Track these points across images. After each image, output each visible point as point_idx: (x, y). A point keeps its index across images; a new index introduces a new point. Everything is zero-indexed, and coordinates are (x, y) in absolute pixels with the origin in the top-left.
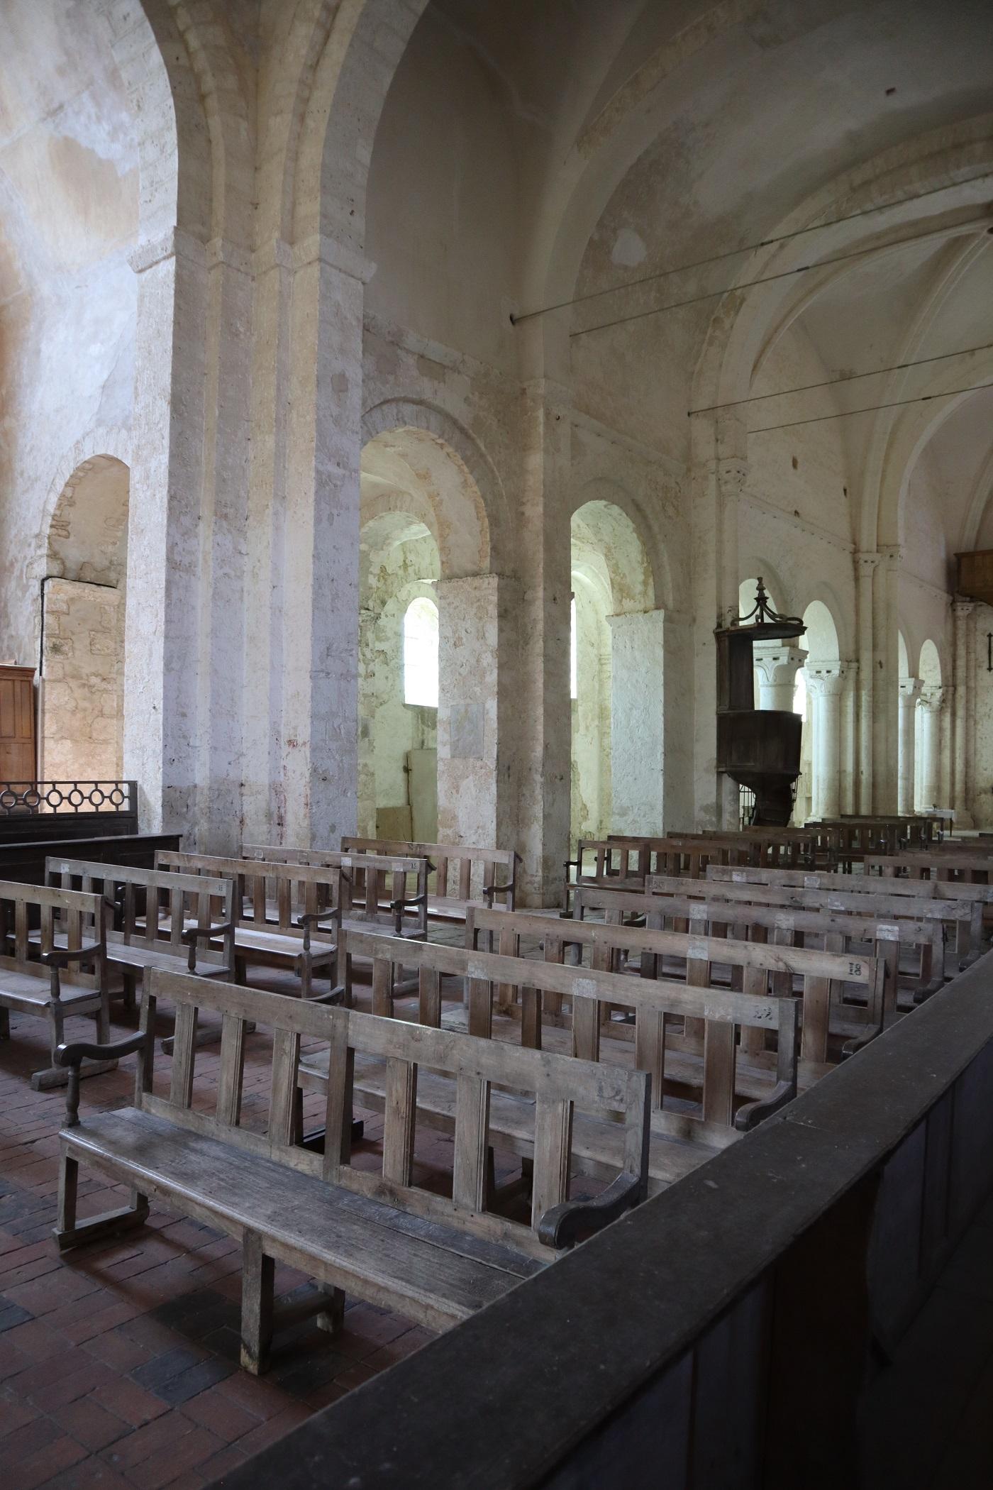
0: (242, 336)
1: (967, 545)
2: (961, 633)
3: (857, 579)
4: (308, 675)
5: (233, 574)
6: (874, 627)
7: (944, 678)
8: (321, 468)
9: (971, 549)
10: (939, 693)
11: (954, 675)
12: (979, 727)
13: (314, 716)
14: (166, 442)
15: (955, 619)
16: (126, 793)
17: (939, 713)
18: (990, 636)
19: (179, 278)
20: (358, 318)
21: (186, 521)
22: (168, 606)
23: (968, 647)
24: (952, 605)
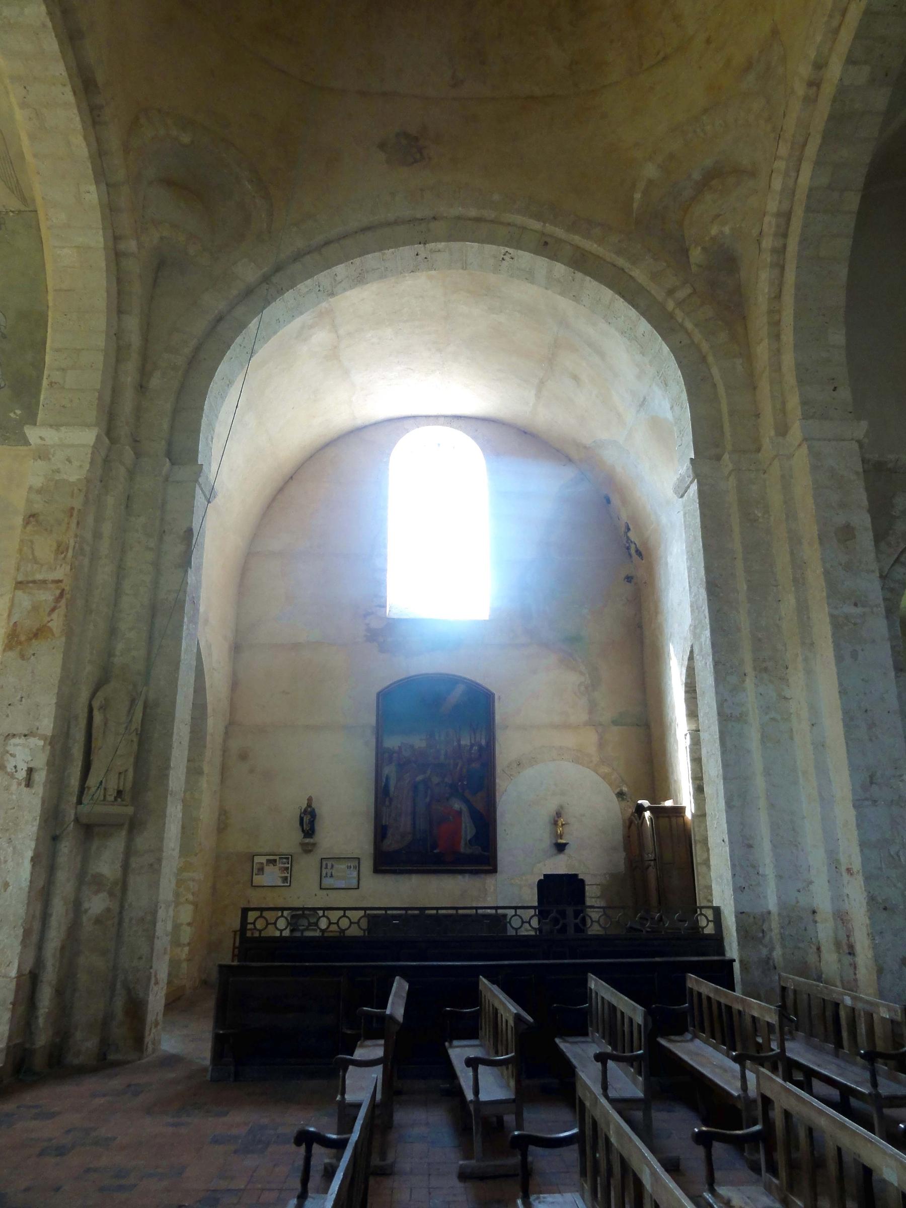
0: (761, 520)
4: (850, 805)
5: (779, 717)
8: (836, 612)
13: (863, 845)
14: (707, 621)
16: (711, 918)
19: (701, 493)
20: (857, 473)
21: (733, 679)
22: (723, 753)
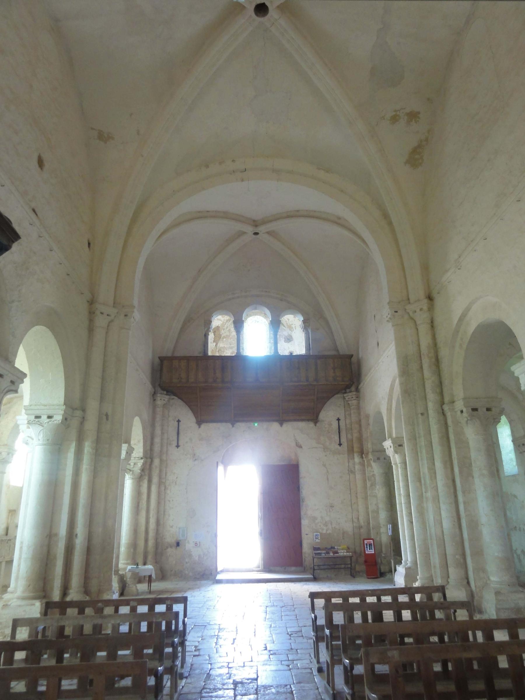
1: (167, 351)
2: (158, 418)
3: (91, 330)
6: (103, 378)
7: (145, 452)
9: (169, 354)
10: (140, 463)
11: (151, 450)
12: (168, 492)
15: (154, 407)
17: (138, 480)
18: (179, 421)
23: (162, 429)
24: (154, 395)
